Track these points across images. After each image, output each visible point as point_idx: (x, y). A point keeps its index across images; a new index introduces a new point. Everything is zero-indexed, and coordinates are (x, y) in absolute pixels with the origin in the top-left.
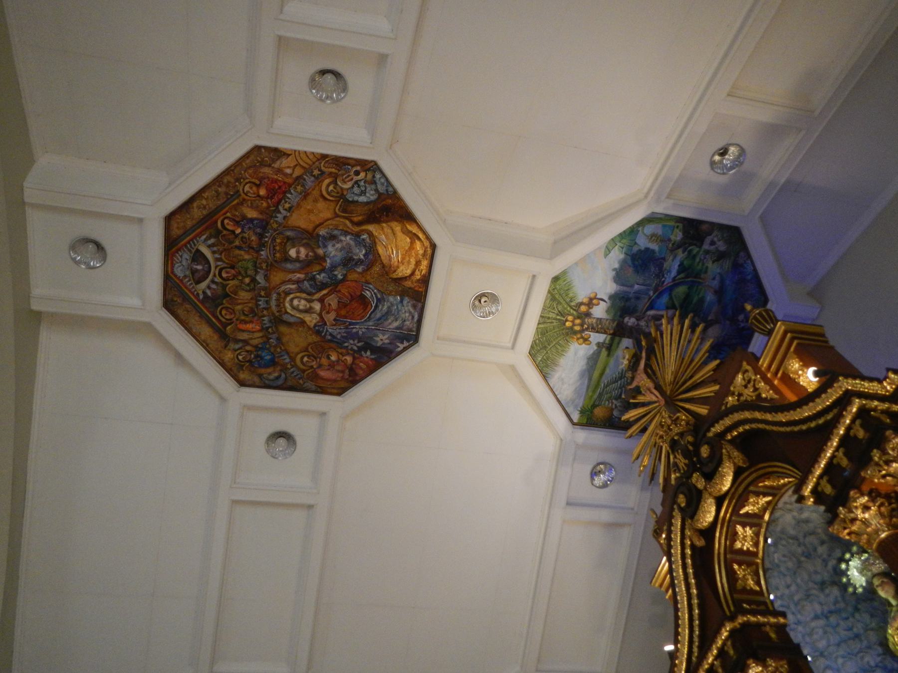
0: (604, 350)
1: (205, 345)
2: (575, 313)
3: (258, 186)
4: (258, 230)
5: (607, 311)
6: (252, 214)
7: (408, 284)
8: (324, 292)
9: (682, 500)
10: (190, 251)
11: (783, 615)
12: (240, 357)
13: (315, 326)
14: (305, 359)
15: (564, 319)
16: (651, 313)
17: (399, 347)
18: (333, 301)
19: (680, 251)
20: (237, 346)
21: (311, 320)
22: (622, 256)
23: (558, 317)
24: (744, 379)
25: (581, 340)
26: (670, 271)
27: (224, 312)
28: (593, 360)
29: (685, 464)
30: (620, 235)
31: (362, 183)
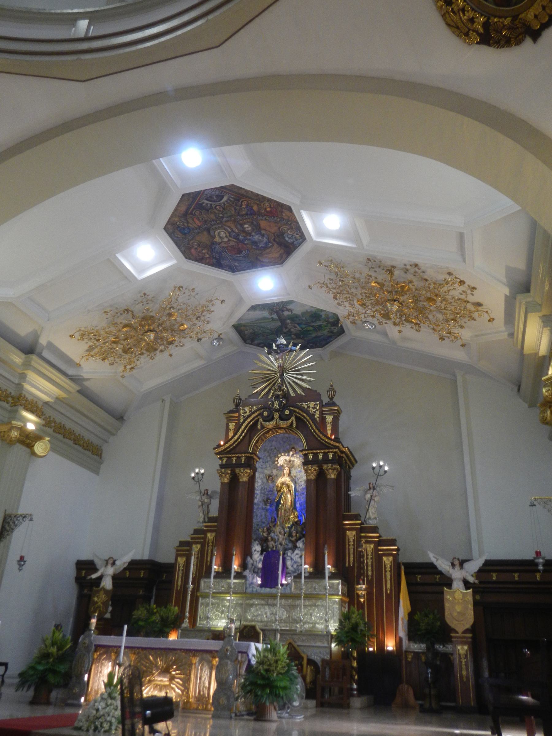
1: (176, 210)
3: (270, 207)
4: (249, 213)
6: (255, 208)
8: (235, 240)
9: (265, 414)
10: (221, 193)
11: (259, 458)
12: (178, 223)
13: (216, 242)
14: (196, 243)
16: (297, 325)
18: (231, 244)
20: (183, 221)
21: (217, 239)
24: (314, 406)
27: (198, 212)
28: (264, 318)
31: (294, 237)
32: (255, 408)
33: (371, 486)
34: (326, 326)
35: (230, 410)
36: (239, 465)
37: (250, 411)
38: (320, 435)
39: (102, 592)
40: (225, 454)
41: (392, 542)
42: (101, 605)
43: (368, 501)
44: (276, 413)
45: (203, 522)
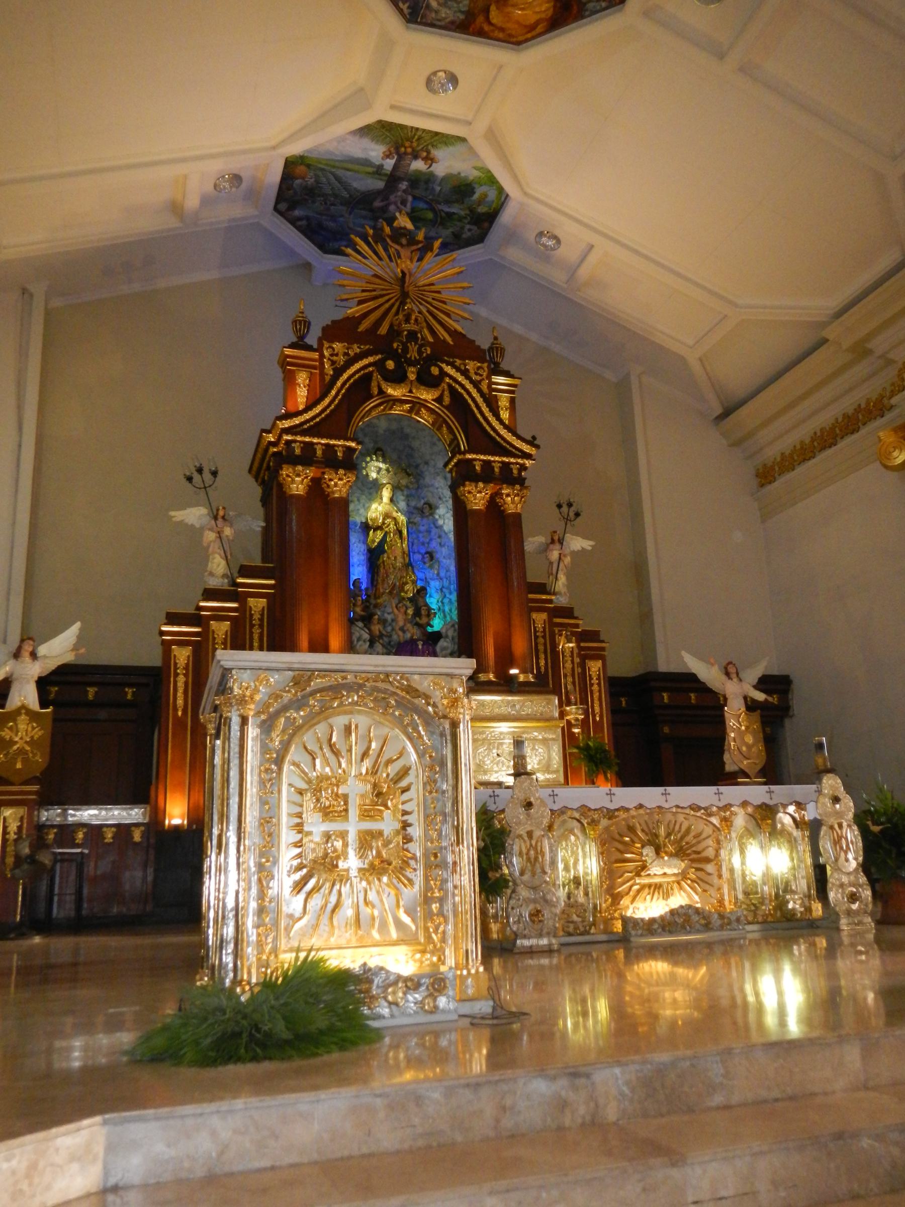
0: (375, 170)
2: (420, 148)
5: (418, 172)
7: (481, 19)
9: (390, 364)
15: (414, 140)
16: (410, 198)
17: (404, 4)
19: (468, 212)
22: (471, 178)
23: (416, 137)
24: (479, 368)
25: (388, 153)
26: (449, 207)
28: (366, 162)
29: (415, 357)
30: (493, 175)
32: (356, 349)
33: (556, 538)
34: (460, 219)
35: (292, 343)
36: (331, 461)
37: (346, 354)
38: (498, 427)
39: (23, 720)
40: (301, 436)
41: (593, 636)
42: (28, 748)
43: (551, 563)
44: (412, 369)
45: (224, 576)
